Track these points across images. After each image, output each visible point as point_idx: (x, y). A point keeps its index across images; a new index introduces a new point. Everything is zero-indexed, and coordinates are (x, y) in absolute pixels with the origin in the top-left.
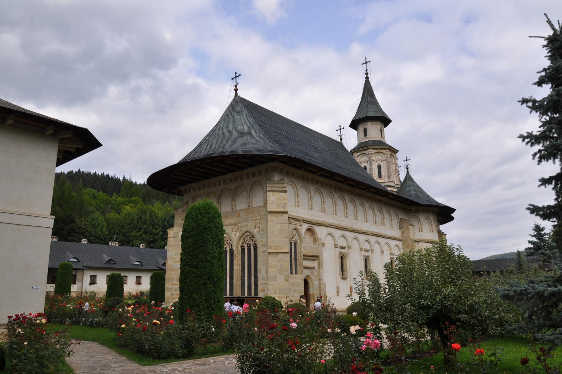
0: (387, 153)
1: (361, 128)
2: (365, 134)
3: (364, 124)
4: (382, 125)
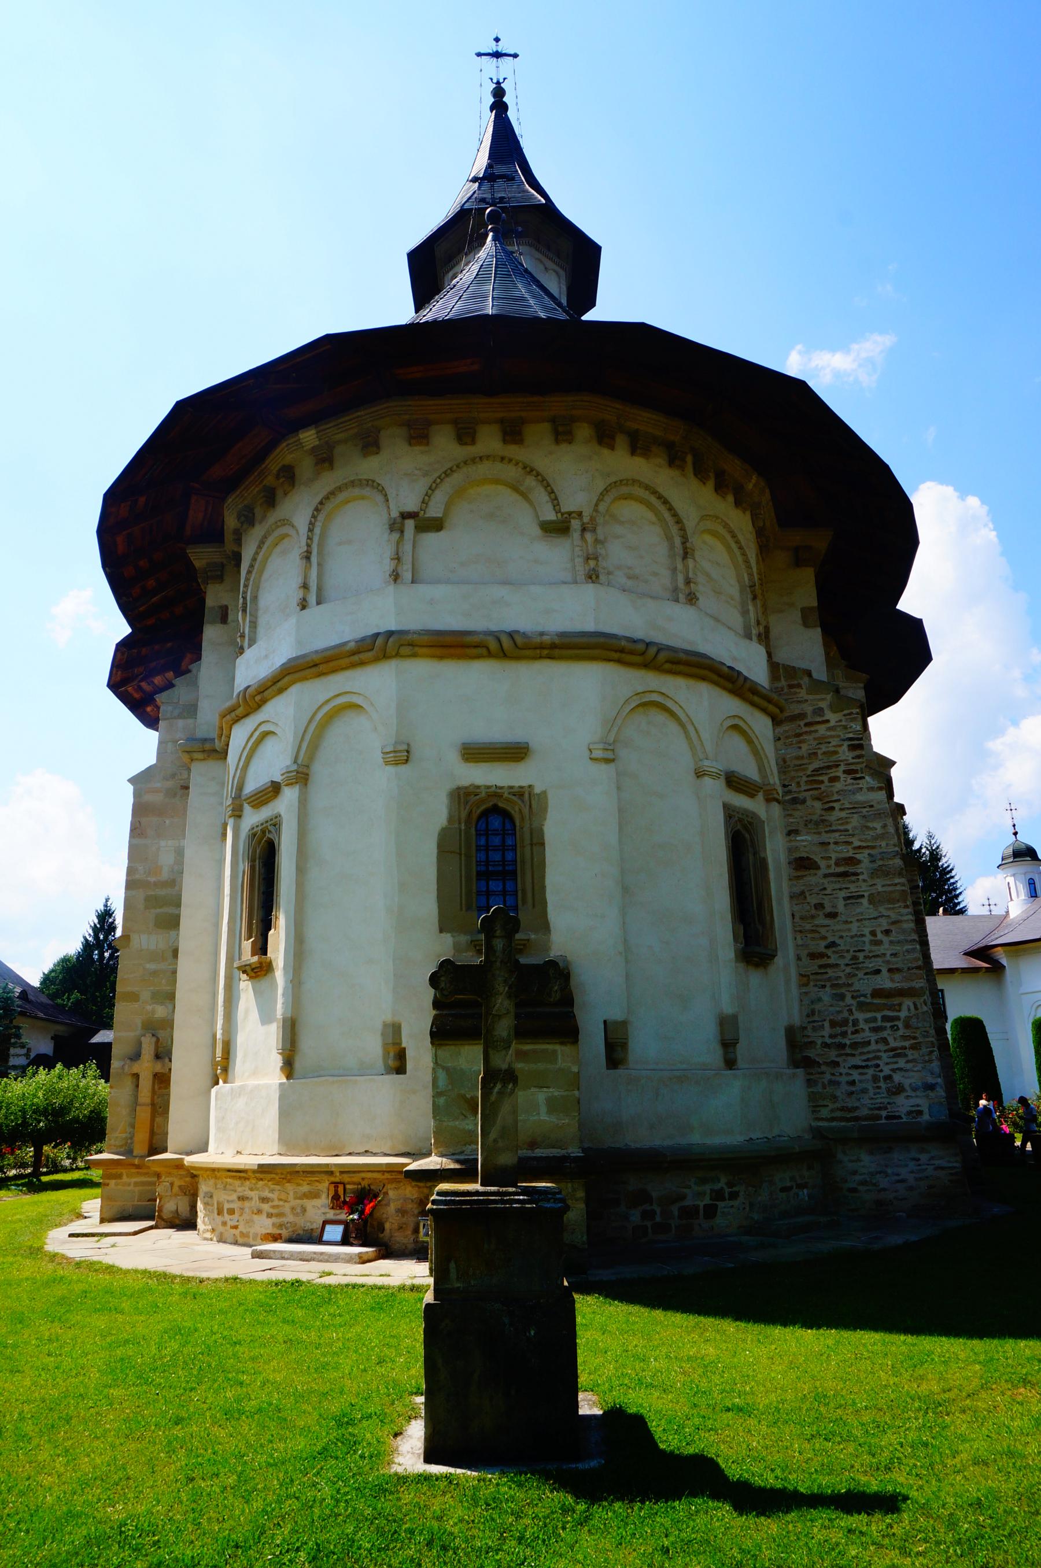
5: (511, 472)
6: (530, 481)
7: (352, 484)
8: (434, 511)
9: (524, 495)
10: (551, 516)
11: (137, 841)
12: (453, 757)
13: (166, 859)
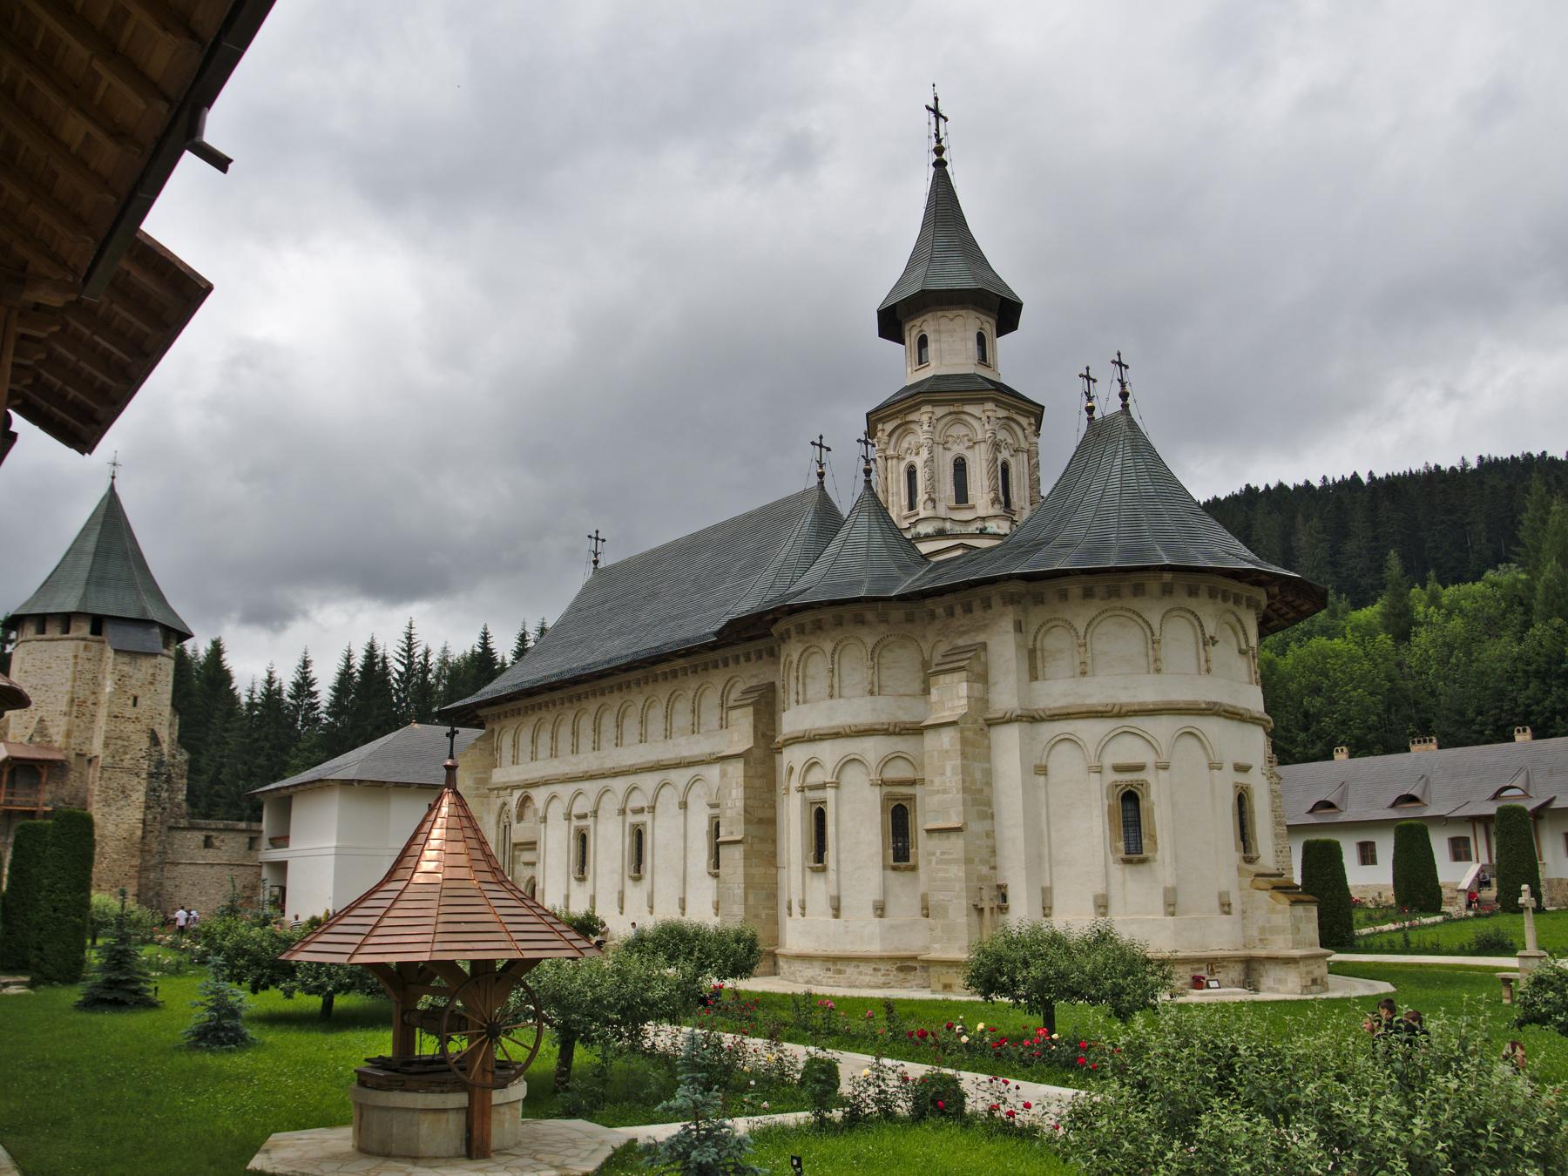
0: (988, 414)
3: (917, 322)
4: (983, 318)
5: (1233, 620)
6: (1238, 627)
7: (1181, 609)
9: (1235, 633)
10: (1244, 647)
11: (964, 762)
12: (1231, 767)
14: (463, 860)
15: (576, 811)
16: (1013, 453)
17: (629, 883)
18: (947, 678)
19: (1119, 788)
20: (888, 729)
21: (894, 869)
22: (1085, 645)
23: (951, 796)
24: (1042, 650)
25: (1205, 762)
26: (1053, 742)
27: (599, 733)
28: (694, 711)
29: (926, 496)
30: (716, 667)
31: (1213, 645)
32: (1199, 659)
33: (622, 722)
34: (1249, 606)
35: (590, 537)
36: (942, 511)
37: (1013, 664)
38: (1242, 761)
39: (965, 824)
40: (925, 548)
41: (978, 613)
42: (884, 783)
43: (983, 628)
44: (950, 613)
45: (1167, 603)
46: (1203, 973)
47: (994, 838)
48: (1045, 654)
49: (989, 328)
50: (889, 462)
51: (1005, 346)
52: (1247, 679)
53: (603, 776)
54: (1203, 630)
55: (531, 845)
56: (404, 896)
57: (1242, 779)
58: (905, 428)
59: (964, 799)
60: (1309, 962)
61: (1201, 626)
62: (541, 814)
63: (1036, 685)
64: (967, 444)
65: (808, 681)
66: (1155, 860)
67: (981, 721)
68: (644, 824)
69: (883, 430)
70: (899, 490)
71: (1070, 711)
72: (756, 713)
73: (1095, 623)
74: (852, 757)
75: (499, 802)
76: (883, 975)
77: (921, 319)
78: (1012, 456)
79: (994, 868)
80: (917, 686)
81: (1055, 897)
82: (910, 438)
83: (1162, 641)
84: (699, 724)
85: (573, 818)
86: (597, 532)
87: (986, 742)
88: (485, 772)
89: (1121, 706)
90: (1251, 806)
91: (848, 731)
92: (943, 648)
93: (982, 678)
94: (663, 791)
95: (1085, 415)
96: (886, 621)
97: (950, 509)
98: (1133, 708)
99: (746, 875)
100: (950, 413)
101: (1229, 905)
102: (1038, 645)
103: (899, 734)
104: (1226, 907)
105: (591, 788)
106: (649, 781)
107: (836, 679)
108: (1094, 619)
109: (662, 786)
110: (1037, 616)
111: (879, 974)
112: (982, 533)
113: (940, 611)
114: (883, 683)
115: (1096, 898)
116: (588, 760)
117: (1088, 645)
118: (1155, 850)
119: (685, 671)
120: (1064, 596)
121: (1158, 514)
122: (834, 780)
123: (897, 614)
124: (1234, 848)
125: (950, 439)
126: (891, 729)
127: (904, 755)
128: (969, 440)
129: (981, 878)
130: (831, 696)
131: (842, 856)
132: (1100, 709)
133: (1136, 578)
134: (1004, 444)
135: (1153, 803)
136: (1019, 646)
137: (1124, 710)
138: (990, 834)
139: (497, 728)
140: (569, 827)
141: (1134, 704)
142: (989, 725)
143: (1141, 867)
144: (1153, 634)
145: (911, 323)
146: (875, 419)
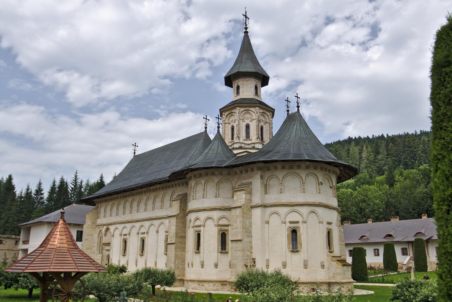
0: (257, 111)
1: (235, 86)
2: (238, 93)
3: (237, 81)
4: (257, 81)
5: (328, 177)
6: (330, 180)
8: (322, 183)
9: (329, 181)
10: (331, 186)
12: (326, 223)
13: (248, 223)
14: (65, 241)
15: (124, 233)
16: (264, 123)
17: (139, 256)
18: (238, 193)
19: (291, 228)
20: (220, 209)
21: (221, 253)
22: (282, 183)
23: (239, 230)
24: (269, 185)
25: (318, 221)
26: (271, 214)
27: (132, 208)
28: (162, 202)
29: (237, 136)
30: (169, 188)
31: (321, 185)
32: (317, 189)
33: (139, 205)
34: (333, 173)
35: (133, 145)
36: (241, 141)
37: (260, 189)
38: (330, 221)
39: (243, 239)
40: (235, 152)
41: (249, 173)
42: (219, 225)
43: (251, 177)
44: (241, 172)
45: (307, 171)
46: (315, 287)
47: (252, 243)
48: (270, 186)
49: (259, 85)
50: (226, 124)
51: (263, 90)
52: (332, 195)
53: (132, 222)
54: (318, 180)
55: (109, 244)
56: (44, 252)
57: (329, 226)
58: (231, 114)
59: (243, 231)
60: (347, 284)
61: (318, 179)
62: (112, 234)
63: (267, 196)
64: (250, 120)
65: (197, 192)
66: (301, 251)
67: (249, 206)
68: (145, 238)
69: (224, 115)
70: (228, 133)
71: (277, 204)
72: (181, 202)
73: (285, 177)
74: (209, 217)
75: (99, 230)
76: (216, 287)
77: (238, 80)
78: (264, 124)
79: (252, 253)
80: (230, 195)
81: (270, 262)
82: (233, 117)
83: (306, 184)
84: (163, 206)
85: (122, 235)
86: (135, 143)
87: (251, 213)
88: (95, 220)
89: (292, 203)
90: (332, 235)
91: (208, 209)
92: (239, 183)
93: (250, 193)
94: (151, 227)
95: (286, 112)
96: (222, 174)
97: (244, 140)
98: (296, 204)
99: (175, 254)
100: (245, 110)
101: (324, 266)
102: (268, 183)
103: (224, 210)
104: (323, 266)
105: (129, 226)
106: (147, 224)
107: (205, 192)
108: (285, 175)
109: (151, 225)
110: (267, 174)
111: (215, 286)
112: (253, 148)
113: (238, 172)
114: (220, 194)
115: (283, 263)
116: (128, 217)
117: (283, 184)
118: (301, 248)
119: (159, 189)
120: (276, 168)
121: (306, 144)
122: (203, 224)
123: (225, 172)
124: (326, 248)
125: (245, 118)
126: (222, 208)
127: (225, 217)
128: (251, 119)
129: (247, 256)
130: (203, 198)
131: (205, 248)
132: (286, 203)
133: (298, 163)
134: (262, 120)
135: (301, 234)
136: (262, 183)
137: (293, 204)
138: (251, 242)
139: (99, 206)
140: (121, 238)
141: (296, 202)
142: (252, 208)
143: (296, 253)
144: (303, 181)
145: (235, 82)
146: (222, 111)
